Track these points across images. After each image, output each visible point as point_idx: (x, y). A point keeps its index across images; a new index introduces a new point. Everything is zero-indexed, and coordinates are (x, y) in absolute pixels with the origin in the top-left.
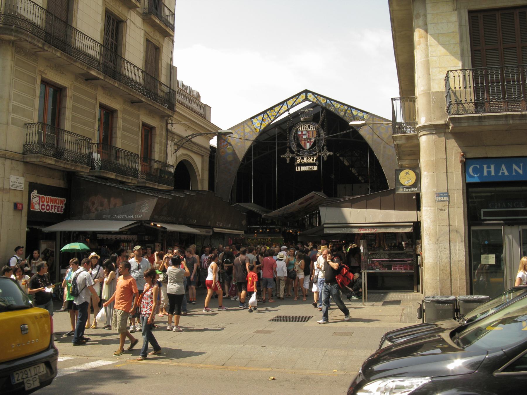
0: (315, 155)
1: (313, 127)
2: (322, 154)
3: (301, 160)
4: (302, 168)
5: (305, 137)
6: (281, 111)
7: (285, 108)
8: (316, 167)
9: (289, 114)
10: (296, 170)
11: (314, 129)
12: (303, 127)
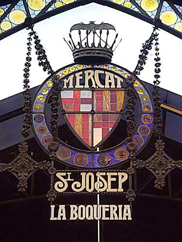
0: (123, 167)
1: (116, 80)
2: (150, 164)
3: (70, 183)
4: (72, 212)
5: (86, 108)
6: (6, 26)
7: (18, 17)
8: (127, 207)
9: (31, 34)
10: (52, 218)
11: (119, 86)
12: (78, 78)
